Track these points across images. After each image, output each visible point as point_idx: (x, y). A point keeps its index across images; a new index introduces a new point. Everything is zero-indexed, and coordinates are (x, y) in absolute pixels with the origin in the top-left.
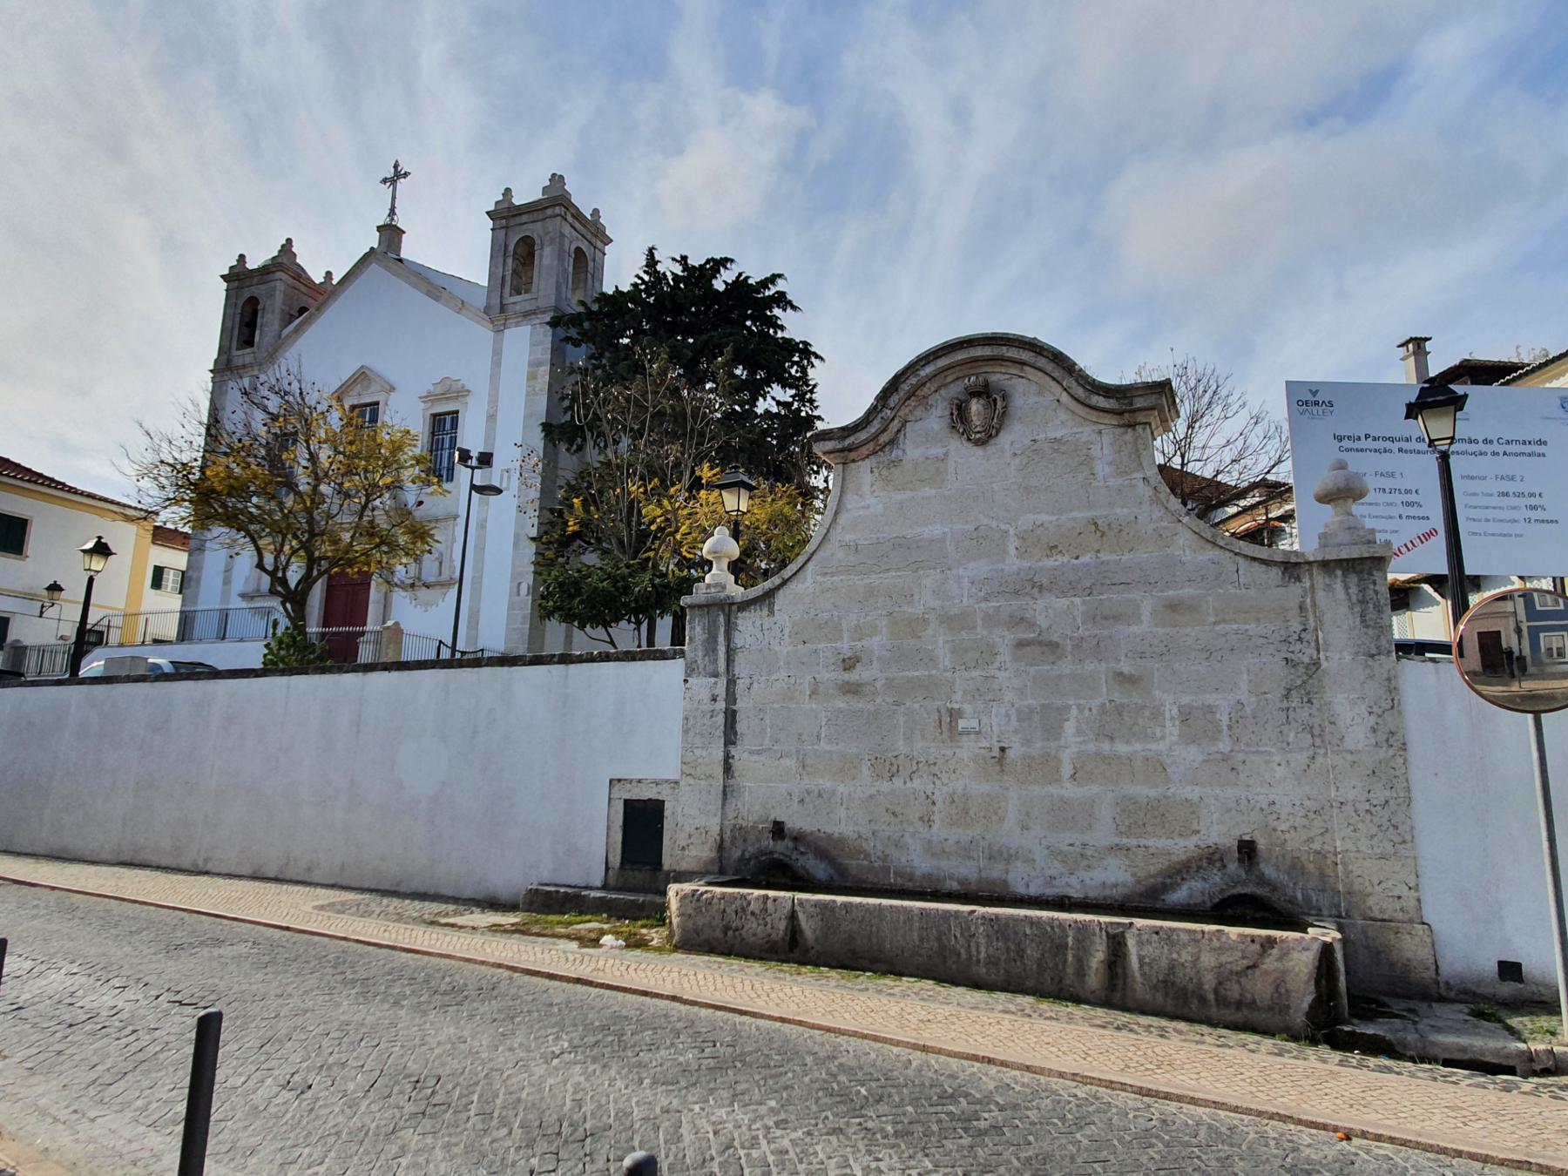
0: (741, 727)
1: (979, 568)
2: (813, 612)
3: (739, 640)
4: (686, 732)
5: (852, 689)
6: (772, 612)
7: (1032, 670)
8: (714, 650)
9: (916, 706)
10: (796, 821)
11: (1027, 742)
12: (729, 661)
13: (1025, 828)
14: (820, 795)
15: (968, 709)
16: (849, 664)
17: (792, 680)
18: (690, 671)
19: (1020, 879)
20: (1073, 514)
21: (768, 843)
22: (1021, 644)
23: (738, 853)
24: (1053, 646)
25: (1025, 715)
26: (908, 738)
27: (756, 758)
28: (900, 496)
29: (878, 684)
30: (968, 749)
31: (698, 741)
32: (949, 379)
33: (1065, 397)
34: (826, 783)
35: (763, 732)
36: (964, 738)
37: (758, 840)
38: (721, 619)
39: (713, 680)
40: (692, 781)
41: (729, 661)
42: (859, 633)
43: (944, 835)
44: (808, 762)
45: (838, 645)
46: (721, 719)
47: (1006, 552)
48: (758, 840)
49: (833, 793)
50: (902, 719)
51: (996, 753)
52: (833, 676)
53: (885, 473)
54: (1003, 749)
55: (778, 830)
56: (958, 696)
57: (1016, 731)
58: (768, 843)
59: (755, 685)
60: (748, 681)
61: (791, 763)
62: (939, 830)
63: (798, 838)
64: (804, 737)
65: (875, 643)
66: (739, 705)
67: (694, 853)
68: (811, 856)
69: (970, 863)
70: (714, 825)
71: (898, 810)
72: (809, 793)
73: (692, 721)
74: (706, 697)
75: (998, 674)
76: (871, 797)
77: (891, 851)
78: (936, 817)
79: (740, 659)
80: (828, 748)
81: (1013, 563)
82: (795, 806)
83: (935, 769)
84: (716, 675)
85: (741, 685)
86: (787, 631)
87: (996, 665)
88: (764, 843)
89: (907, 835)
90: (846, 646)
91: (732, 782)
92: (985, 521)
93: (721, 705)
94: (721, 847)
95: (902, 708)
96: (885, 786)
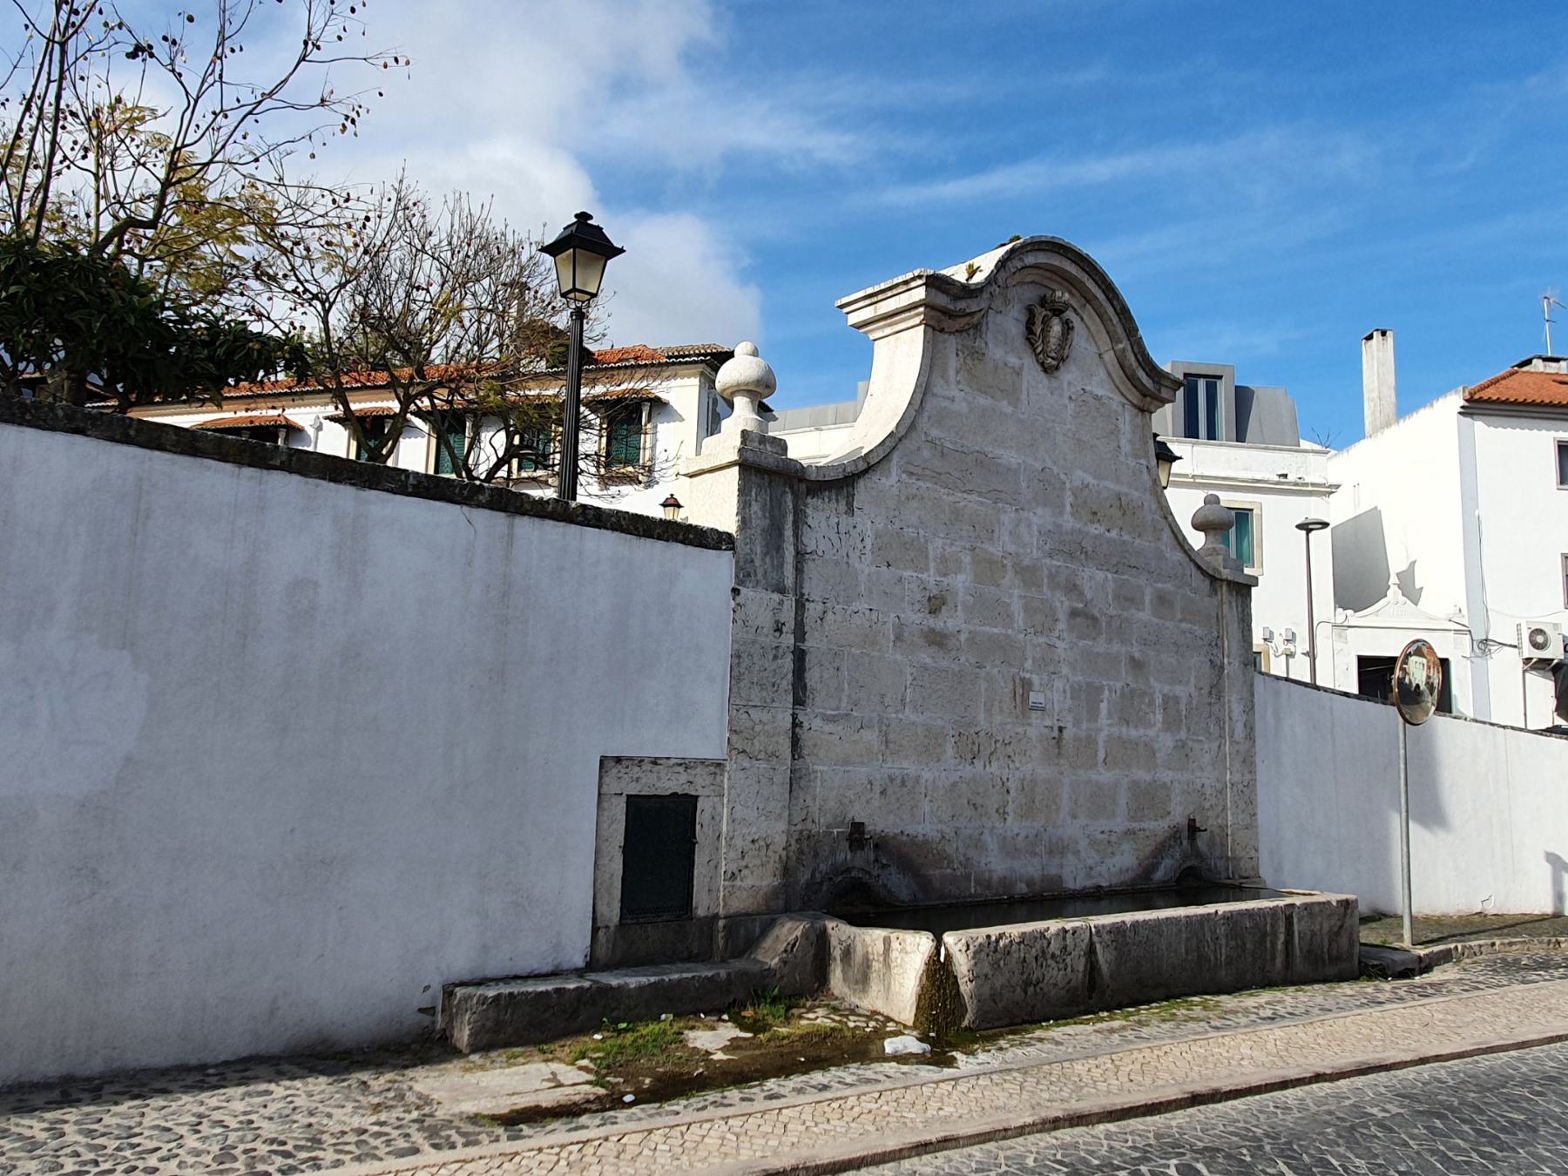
0: (812, 677)
1: (1041, 517)
2: (898, 525)
3: (810, 541)
4: (736, 678)
5: (937, 640)
6: (850, 510)
7: (1081, 643)
8: (779, 549)
9: (995, 671)
10: (880, 822)
11: (1077, 723)
12: (799, 570)
13: (1074, 817)
14: (903, 783)
15: (1036, 679)
16: (935, 604)
17: (875, 614)
18: (744, 575)
19: (1074, 877)
20: (1106, 483)
21: (844, 854)
22: (1074, 613)
23: (807, 876)
24: (1094, 619)
25: (1076, 692)
26: (989, 711)
27: (828, 728)
28: (983, 401)
29: (963, 637)
30: (1037, 727)
31: (756, 696)
32: (1029, 279)
33: (1109, 356)
34: (909, 766)
35: (840, 689)
36: (1034, 714)
37: (833, 852)
38: (789, 498)
39: (776, 596)
40: (746, 764)
41: (799, 570)
42: (947, 565)
43: (1016, 830)
44: (891, 736)
45: (924, 576)
46: (788, 662)
47: (1063, 506)
48: (833, 852)
49: (918, 779)
50: (984, 686)
51: (1056, 733)
52: (917, 618)
53: (969, 361)
54: (1061, 729)
55: (857, 834)
56: (1028, 664)
57: (1070, 710)
58: (844, 854)
59: (830, 616)
60: (820, 607)
61: (871, 736)
62: (1013, 825)
63: (881, 844)
64: (887, 700)
65: (961, 582)
66: (810, 643)
67: (749, 882)
68: (893, 870)
69: (1036, 861)
70: (777, 831)
71: (979, 801)
72: (892, 780)
73: (746, 662)
74: (766, 620)
75: (1058, 643)
76: (954, 785)
77: (972, 853)
78: (1009, 809)
79: (810, 568)
80: (913, 717)
81: (1068, 522)
82: (877, 802)
83: (1009, 750)
84: (782, 590)
85: (813, 610)
86: (868, 542)
87: (1057, 633)
88: (840, 857)
89: (986, 831)
90: (932, 580)
91: (799, 763)
92: (1049, 464)
93: (788, 640)
94: (787, 871)
95: (983, 673)
96: (967, 771)
